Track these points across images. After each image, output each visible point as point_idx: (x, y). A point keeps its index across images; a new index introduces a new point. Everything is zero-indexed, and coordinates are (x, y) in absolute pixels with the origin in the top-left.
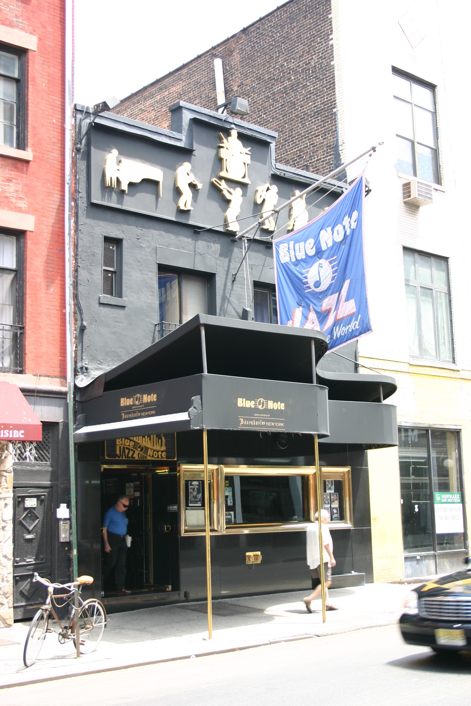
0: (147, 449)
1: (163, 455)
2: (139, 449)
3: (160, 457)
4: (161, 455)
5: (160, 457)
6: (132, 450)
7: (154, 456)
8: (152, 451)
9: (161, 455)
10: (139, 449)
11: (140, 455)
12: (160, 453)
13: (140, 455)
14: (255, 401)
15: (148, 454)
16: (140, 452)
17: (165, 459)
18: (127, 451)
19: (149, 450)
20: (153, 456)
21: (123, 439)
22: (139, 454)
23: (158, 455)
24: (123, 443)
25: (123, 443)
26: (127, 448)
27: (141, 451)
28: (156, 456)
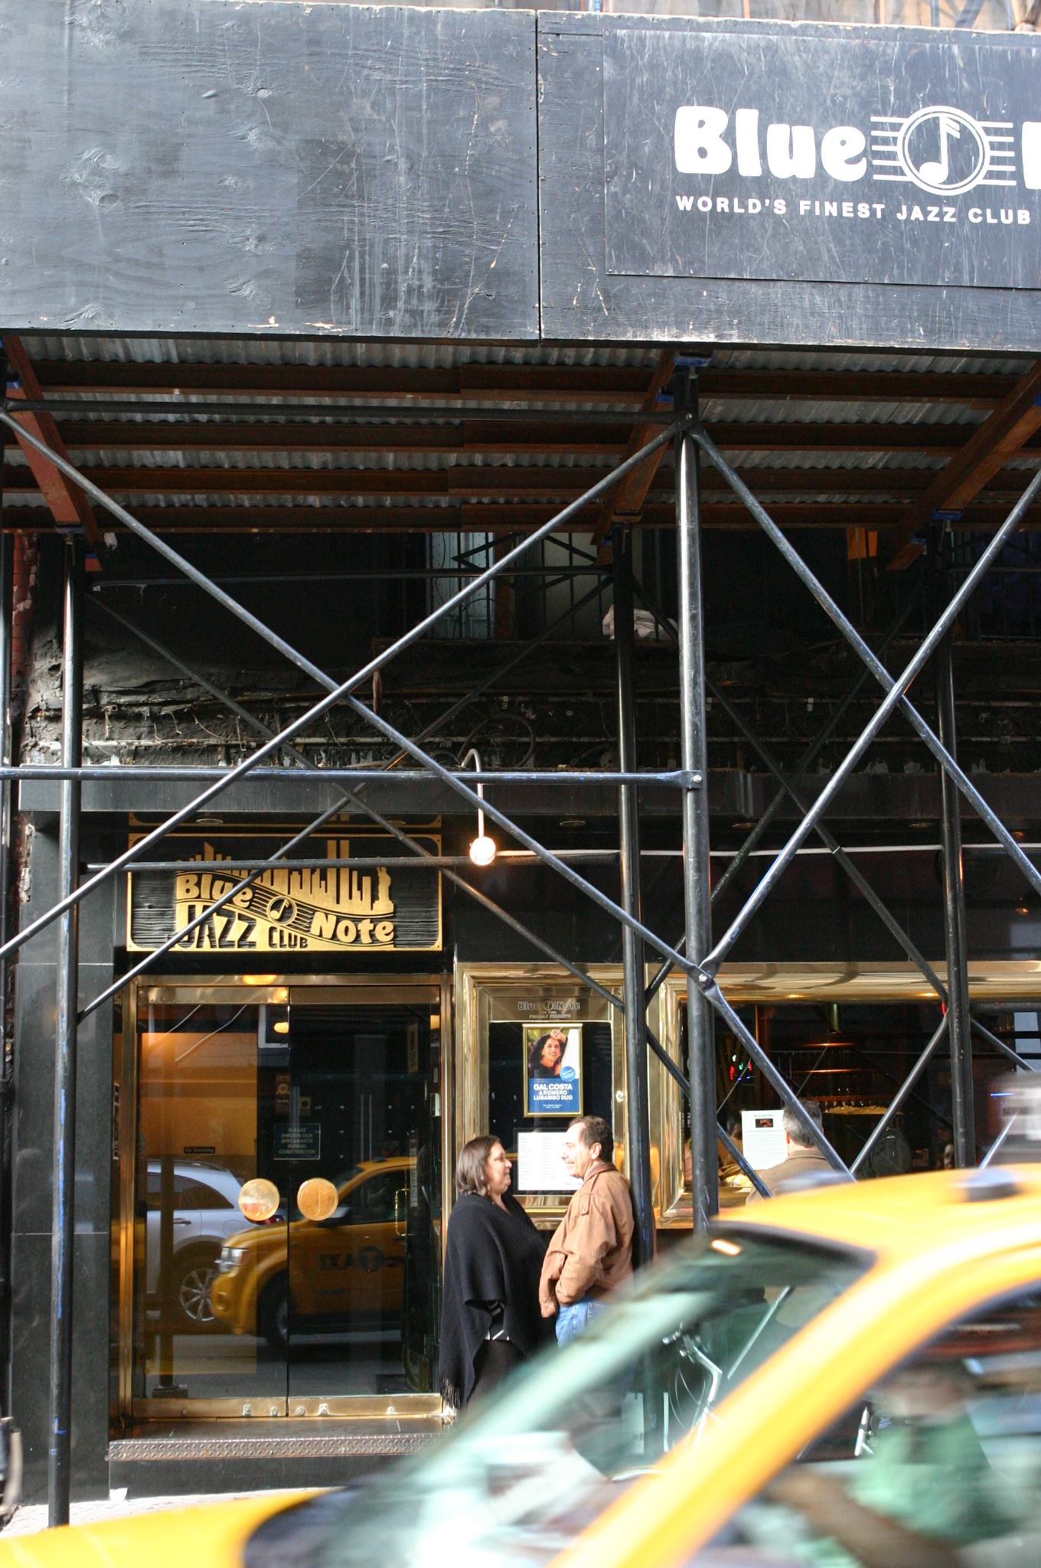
0: (308, 912)
1: (380, 935)
2: (276, 914)
3: (365, 938)
4: (372, 934)
5: (365, 938)
6: (241, 917)
7: (340, 934)
8: (333, 919)
9: (372, 934)
10: (276, 914)
11: (276, 936)
12: (365, 926)
13: (276, 936)
14: (866, 127)
15: (315, 930)
16: (277, 925)
17: (391, 948)
18: (219, 922)
19: (319, 917)
20: (334, 937)
21: (206, 880)
22: (272, 929)
23: (358, 931)
24: (205, 895)
25: (205, 895)
26: (219, 911)
27: (280, 920)
28: (352, 936)
